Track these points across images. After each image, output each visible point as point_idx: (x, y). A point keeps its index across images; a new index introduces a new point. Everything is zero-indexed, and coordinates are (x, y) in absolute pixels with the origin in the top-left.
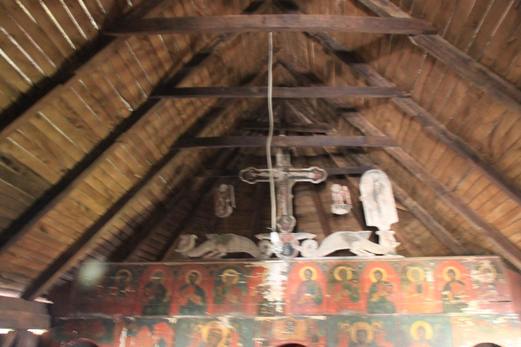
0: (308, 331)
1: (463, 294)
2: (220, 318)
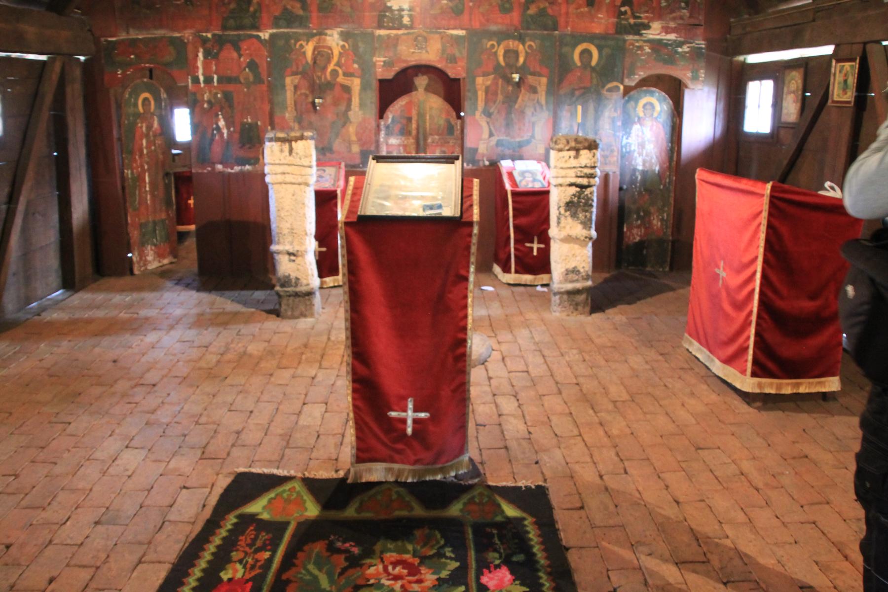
0: (444, 50)
1: (647, 12)
2: (329, 32)
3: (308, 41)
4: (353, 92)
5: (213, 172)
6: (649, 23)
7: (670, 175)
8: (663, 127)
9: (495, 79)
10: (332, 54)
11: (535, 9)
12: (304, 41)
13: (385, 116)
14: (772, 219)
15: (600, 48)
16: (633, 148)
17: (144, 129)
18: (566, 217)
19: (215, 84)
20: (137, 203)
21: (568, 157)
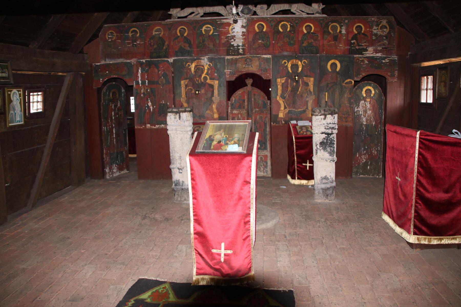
0: (260, 65)
1: (365, 42)
2: (202, 58)
3: (192, 63)
4: (215, 87)
5: (145, 129)
6: (366, 48)
7: (381, 126)
8: (376, 101)
9: (286, 79)
10: (204, 69)
11: (307, 43)
12: (190, 63)
13: (231, 99)
14: (421, 150)
15: (341, 62)
16: (361, 113)
17: (113, 107)
18: (320, 150)
19: (147, 85)
20: (109, 143)
21: (320, 119)
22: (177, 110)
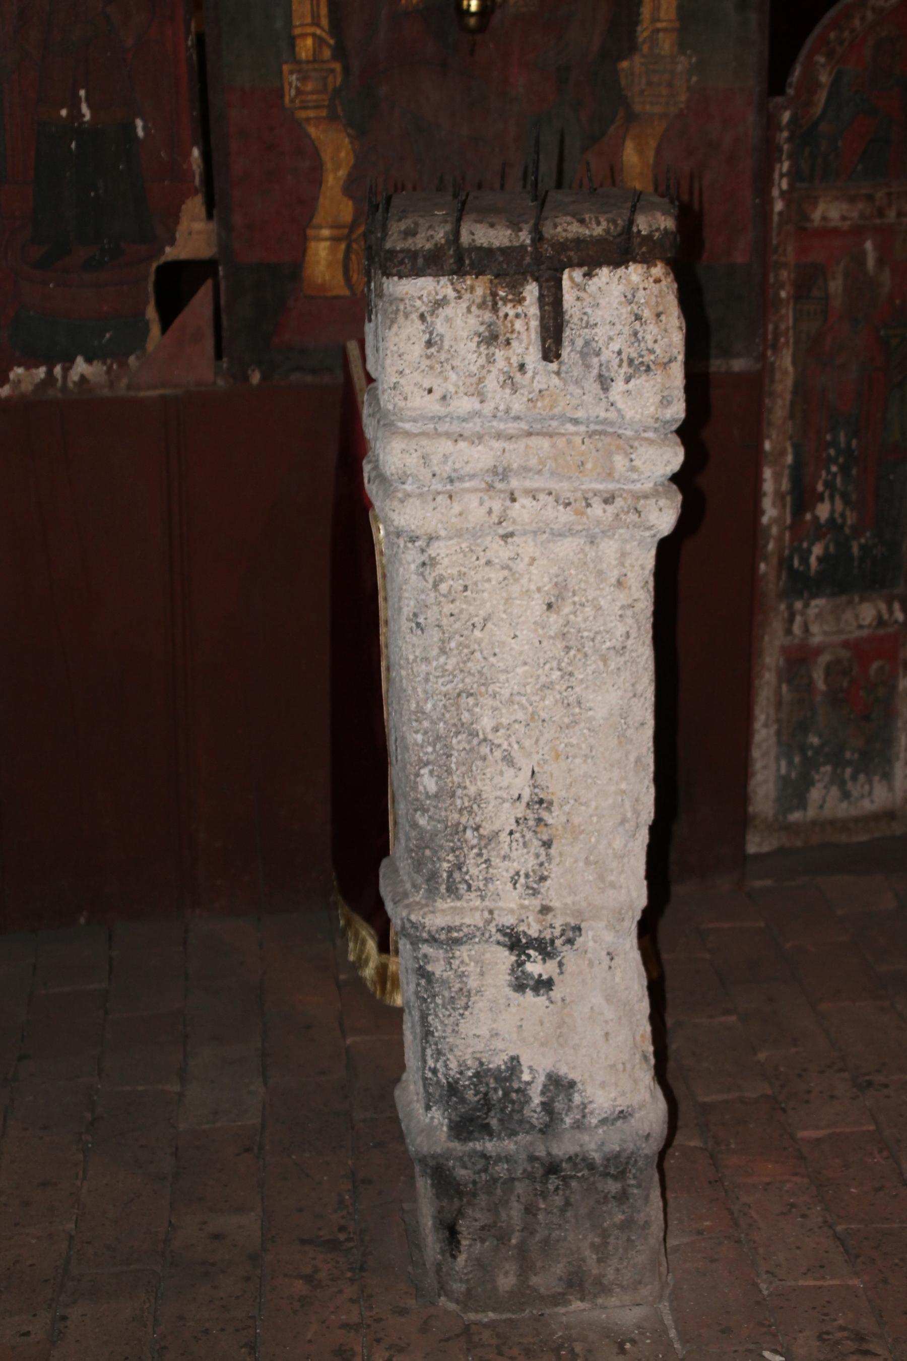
22: (525, 237)
